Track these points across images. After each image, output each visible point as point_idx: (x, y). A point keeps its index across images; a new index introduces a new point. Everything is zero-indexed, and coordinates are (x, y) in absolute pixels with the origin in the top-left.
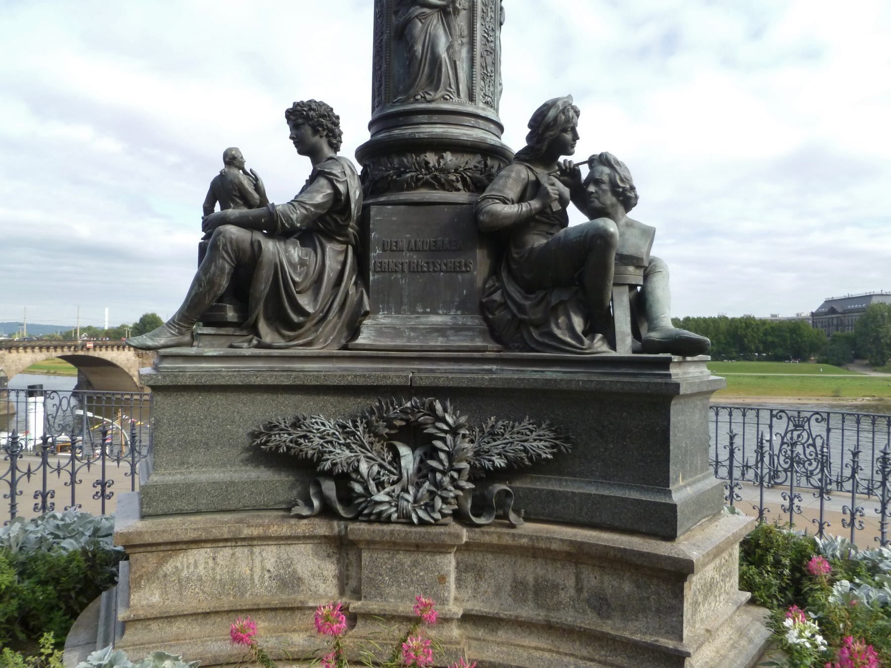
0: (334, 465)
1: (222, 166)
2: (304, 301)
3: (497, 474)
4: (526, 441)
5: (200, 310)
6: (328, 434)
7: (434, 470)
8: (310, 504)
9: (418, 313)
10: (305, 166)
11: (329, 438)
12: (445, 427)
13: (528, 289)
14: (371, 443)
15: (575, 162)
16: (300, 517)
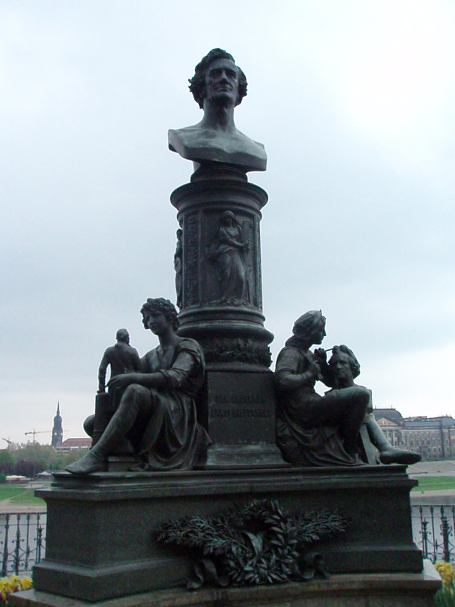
0: (215, 549)
1: (116, 342)
3: (313, 545)
4: (327, 522)
6: (206, 529)
7: (275, 547)
9: (239, 444)
11: (207, 532)
12: (278, 518)
14: (233, 533)
15: (325, 349)
16: (192, 590)
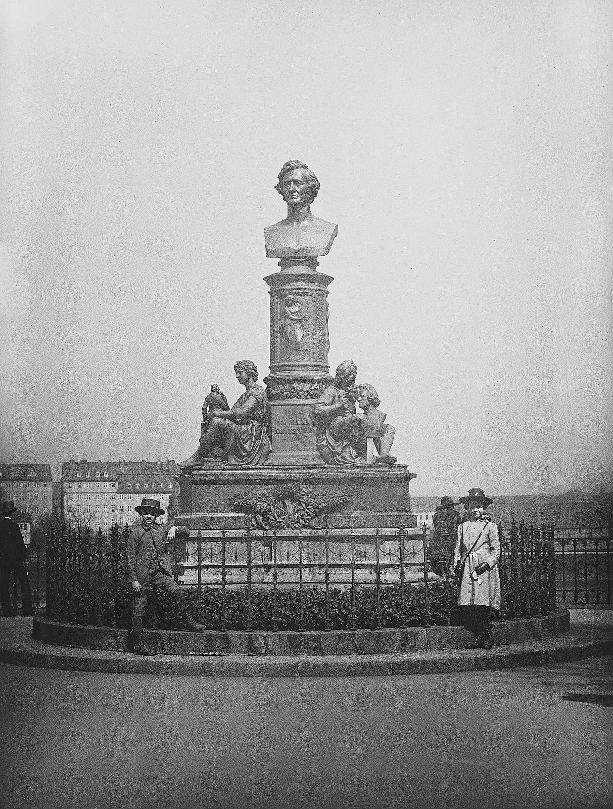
2: (247, 446)
5: (204, 452)
8: (252, 525)
10: (243, 389)
12: (304, 493)
13: (336, 439)
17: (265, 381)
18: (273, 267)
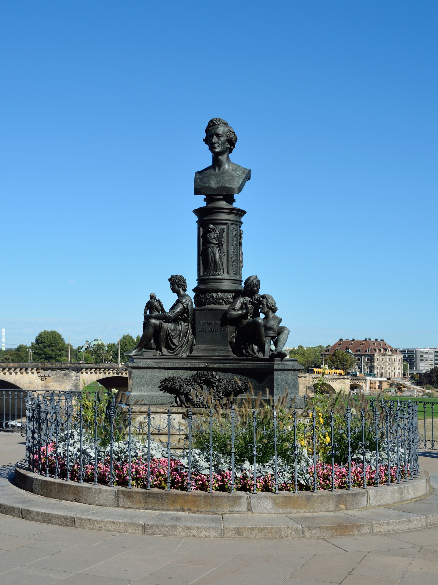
0: (184, 390)
1: (149, 299)
2: (175, 341)
17: (194, 290)
18: (200, 202)
